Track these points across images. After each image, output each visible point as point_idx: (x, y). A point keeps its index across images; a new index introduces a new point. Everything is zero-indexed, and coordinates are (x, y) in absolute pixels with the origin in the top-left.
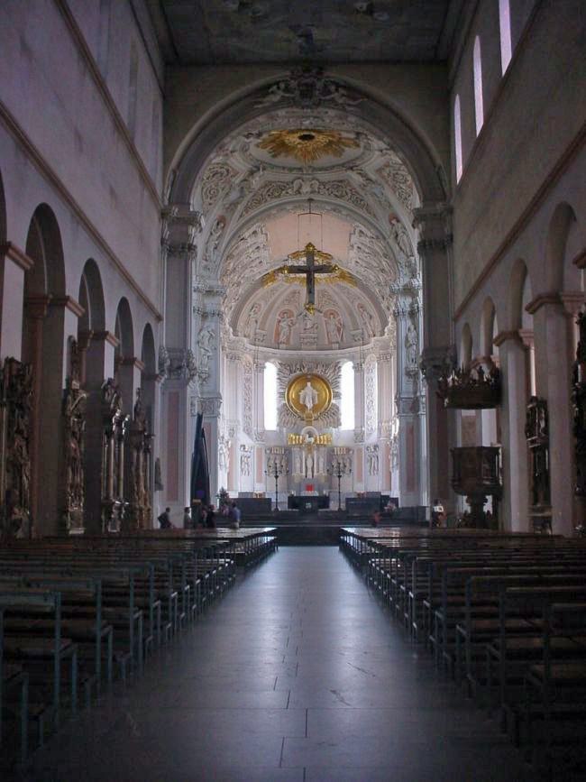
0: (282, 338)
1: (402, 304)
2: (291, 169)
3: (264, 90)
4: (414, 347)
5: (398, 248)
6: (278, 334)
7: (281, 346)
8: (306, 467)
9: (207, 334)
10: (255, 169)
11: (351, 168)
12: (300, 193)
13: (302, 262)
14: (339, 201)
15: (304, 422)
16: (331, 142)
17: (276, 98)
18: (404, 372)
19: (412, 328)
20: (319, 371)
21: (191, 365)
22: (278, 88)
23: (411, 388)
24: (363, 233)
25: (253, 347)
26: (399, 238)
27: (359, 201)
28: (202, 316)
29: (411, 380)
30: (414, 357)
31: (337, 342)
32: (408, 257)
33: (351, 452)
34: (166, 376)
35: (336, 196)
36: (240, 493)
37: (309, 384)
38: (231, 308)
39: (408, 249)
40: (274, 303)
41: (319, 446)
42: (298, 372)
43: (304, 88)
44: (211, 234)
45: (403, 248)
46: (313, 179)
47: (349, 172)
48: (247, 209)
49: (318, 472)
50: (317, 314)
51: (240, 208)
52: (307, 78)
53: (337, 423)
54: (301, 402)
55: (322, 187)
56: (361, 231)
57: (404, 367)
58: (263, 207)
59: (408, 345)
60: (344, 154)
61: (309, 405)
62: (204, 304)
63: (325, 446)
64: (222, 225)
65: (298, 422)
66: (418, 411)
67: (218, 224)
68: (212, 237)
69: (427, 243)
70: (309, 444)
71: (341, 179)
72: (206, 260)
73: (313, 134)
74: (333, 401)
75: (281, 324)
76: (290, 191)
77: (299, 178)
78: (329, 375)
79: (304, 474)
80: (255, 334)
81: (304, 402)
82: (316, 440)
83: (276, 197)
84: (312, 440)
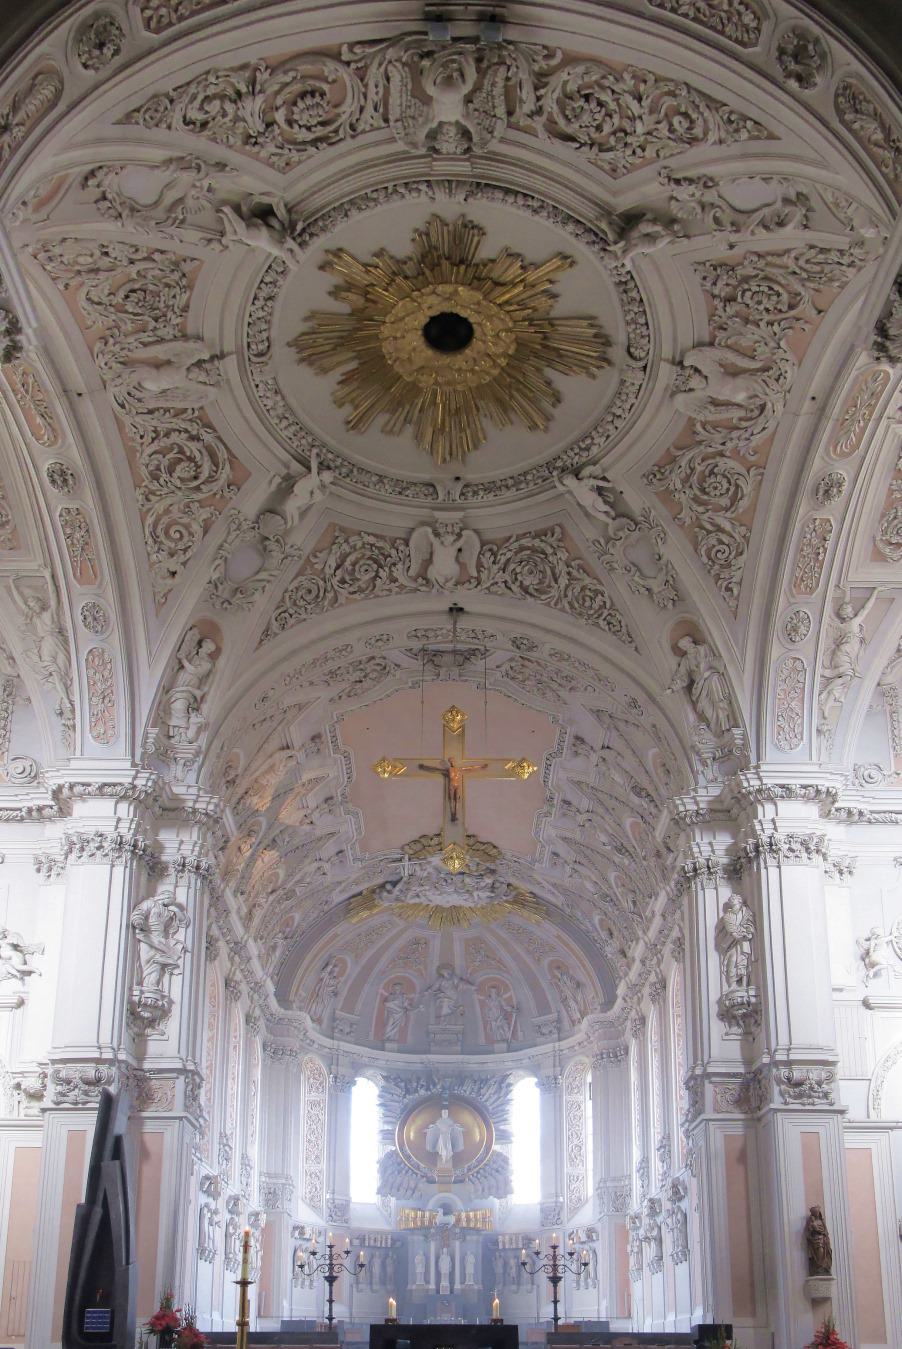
0: (391, 1031)
5: (692, 717)
6: (382, 1023)
7: (388, 1045)
15: (435, 1187)
24: (582, 741)
25: (328, 1042)
26: (696, 691)
31: (504, 1040)
32: (720, 734)
39: (722, 716)
40: (375, 959)
45: (709, 713)
50: (463, 986)
53: (503, 1189)
63: (478, 1231)
65: (421, 1185)
70: (444, 1227)
71: (542, 526)
75: (390, 1005)
82: (458, 1220)
84: (451, 1219)
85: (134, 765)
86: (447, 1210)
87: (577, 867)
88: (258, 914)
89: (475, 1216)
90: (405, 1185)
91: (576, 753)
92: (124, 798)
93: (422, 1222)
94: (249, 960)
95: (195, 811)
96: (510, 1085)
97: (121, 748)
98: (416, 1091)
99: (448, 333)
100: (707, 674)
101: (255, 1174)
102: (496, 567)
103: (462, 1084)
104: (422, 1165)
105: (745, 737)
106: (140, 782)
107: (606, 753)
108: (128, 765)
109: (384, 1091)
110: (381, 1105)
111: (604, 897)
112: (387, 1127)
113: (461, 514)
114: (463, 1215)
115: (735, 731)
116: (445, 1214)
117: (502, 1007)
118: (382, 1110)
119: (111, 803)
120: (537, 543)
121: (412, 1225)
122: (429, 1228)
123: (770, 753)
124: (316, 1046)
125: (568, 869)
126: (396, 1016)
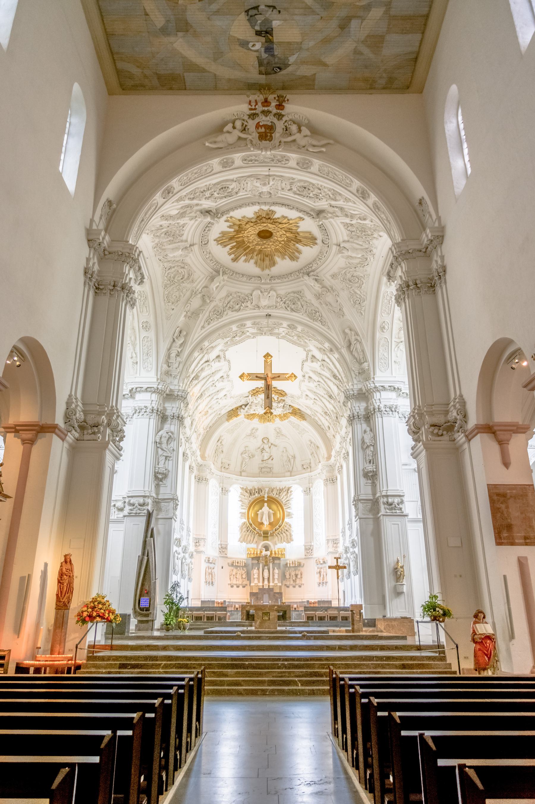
1: (357, 408)
2: (250, 277)
3: (220, 129)
4: (372, 448)
7: (243, 474)
8: (263, 579)
9: (165, 434)
10: (214, 273)
11: (308, 274)
12: (259, 307)
13: (260, 370)
14: (295, 316)
16: (289, 240)
17: (231, 138)
18: (362, 473)
19: (368, 429)
20: (274, 495)
21: (114, 423)
22: (234, 128)
23: (369, 490)
27: (314, 315)
28: (162, 418)
29: (370, 482)
30: (371, 458)
33: (302, 565)
34: (77, 435)
35: (292, 310)
36: (202, 602)
37: (266, 504)
38: (199, 435)
39: (361, 357)
41: (274, 559)
42: (257, 495)
43: (263, 130)
44: (174, 341)
45: (356, 355)
46: (271, 289)
47: (306, 277)
48: (209, 321)
49: (273, 582)
51: (203, 317)
52: (266, 113)
53: (289, 540)
54: (259, 520)
55: (279, 300)
56: (313, 356)
57: (361, 468)
58: (225, 319)
59: (365, 447)
60: (301, 256)
61: (266, 523)
62: (164, 407)
64: (185, 333)
66: (378, 513)
67: (180, 332)
68: (174, 344)
69: (411, 283)
70: (266, 556)
72: (169, 367)
73: (271, 227)
74: (286, 520)
75: (244, 455)
76: (249, 304)
77: (257, 288)
78: (283, 498)
79: (261, 584)
80: (222, 463)
81: (262, 519)
82: (271, 554)
83: (236, 310)
85: (158, 379)
86: (267, 548)
87: (315, 401)
88: (195, 423)
89: (278, 552)
90: (250, 536)
91: (312, 362)
92: (154, 392)
93: (257, 554)
94: (191, 443)
95: (178, 395)
96: (291, 492)
97: (153, 373)
98: (254, 494)
99: (265, 235)
100: (355, 342)
101: (191, 534)
102: (282, 302)
103: (272, 491)
104: (257, 528)
105: (369, 366)
106: (160, 387)
107: (324, 363)
108: (155, 380)
109: (242, 494)
110: (240, 501)
111: (326, 413)
112: (244, 511)
113: (269, 286)
114: (273, 551)
115: (365, 363)
116: (266, 551)
117: (288, 457)
118: (240, 503)
119: (149, 394)
120: (296, 295)
121: (252, 556)
122: (259, 557)
123: (378, 373)
124: (214, 475)
125: (312, 401)
126: (246, 460)
